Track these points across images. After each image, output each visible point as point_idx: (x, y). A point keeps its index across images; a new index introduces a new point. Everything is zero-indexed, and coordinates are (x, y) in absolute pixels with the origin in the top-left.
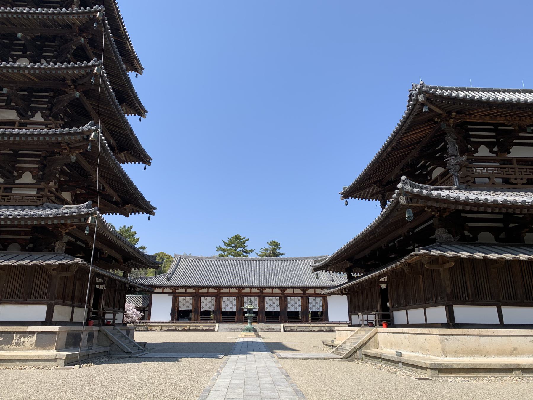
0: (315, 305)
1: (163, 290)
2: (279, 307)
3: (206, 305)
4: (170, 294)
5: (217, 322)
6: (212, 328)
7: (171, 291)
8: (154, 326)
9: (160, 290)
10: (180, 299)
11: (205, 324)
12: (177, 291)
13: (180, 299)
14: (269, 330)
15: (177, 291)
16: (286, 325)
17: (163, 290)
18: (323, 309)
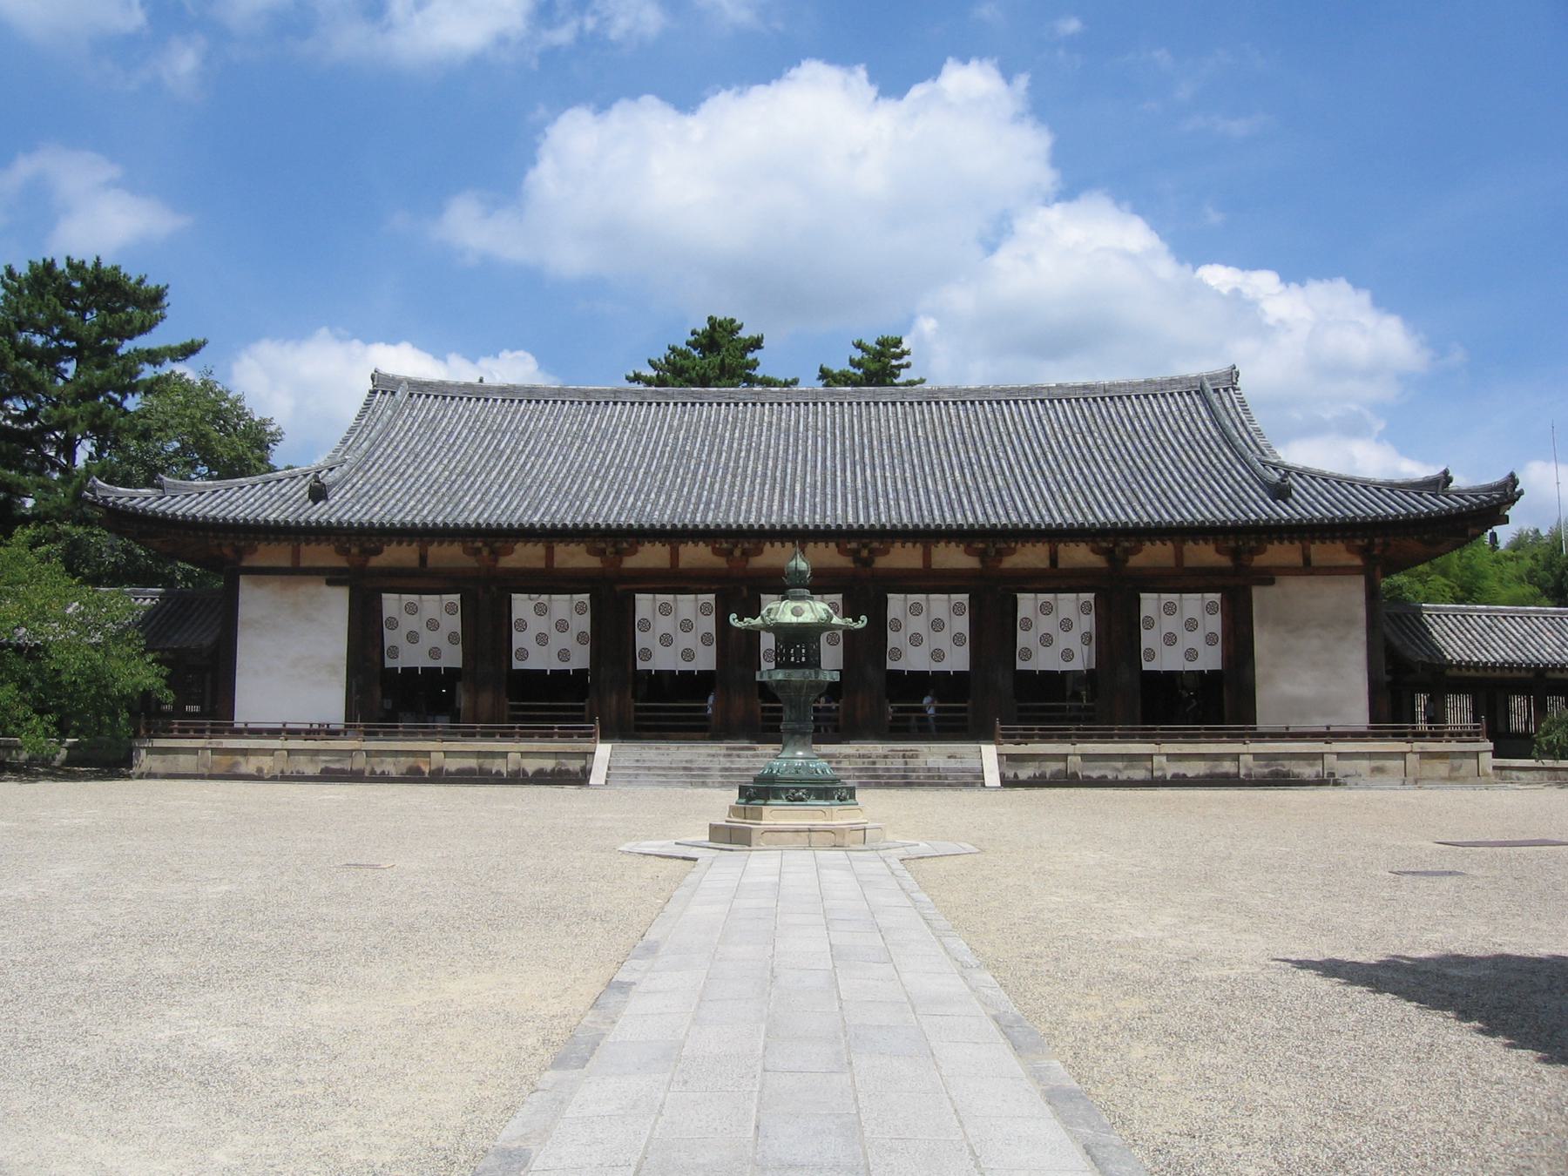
0: (1180, 634)
1: (296, 554)
2: (965, 650)
3: (542, 639)
4: (334, 578)
5: (605, 737)
6: (575, 765)
7: (341, 562)
8: (245, 752)
9: (278, 555)
10: (392, 604)
11: (535, 746)
12: (375, 562)
13: (392, 604)
14: (906, 781)
15: (375, 562)
16: (1010, 748)
17: (296, 554)
18: (1227, 657)
